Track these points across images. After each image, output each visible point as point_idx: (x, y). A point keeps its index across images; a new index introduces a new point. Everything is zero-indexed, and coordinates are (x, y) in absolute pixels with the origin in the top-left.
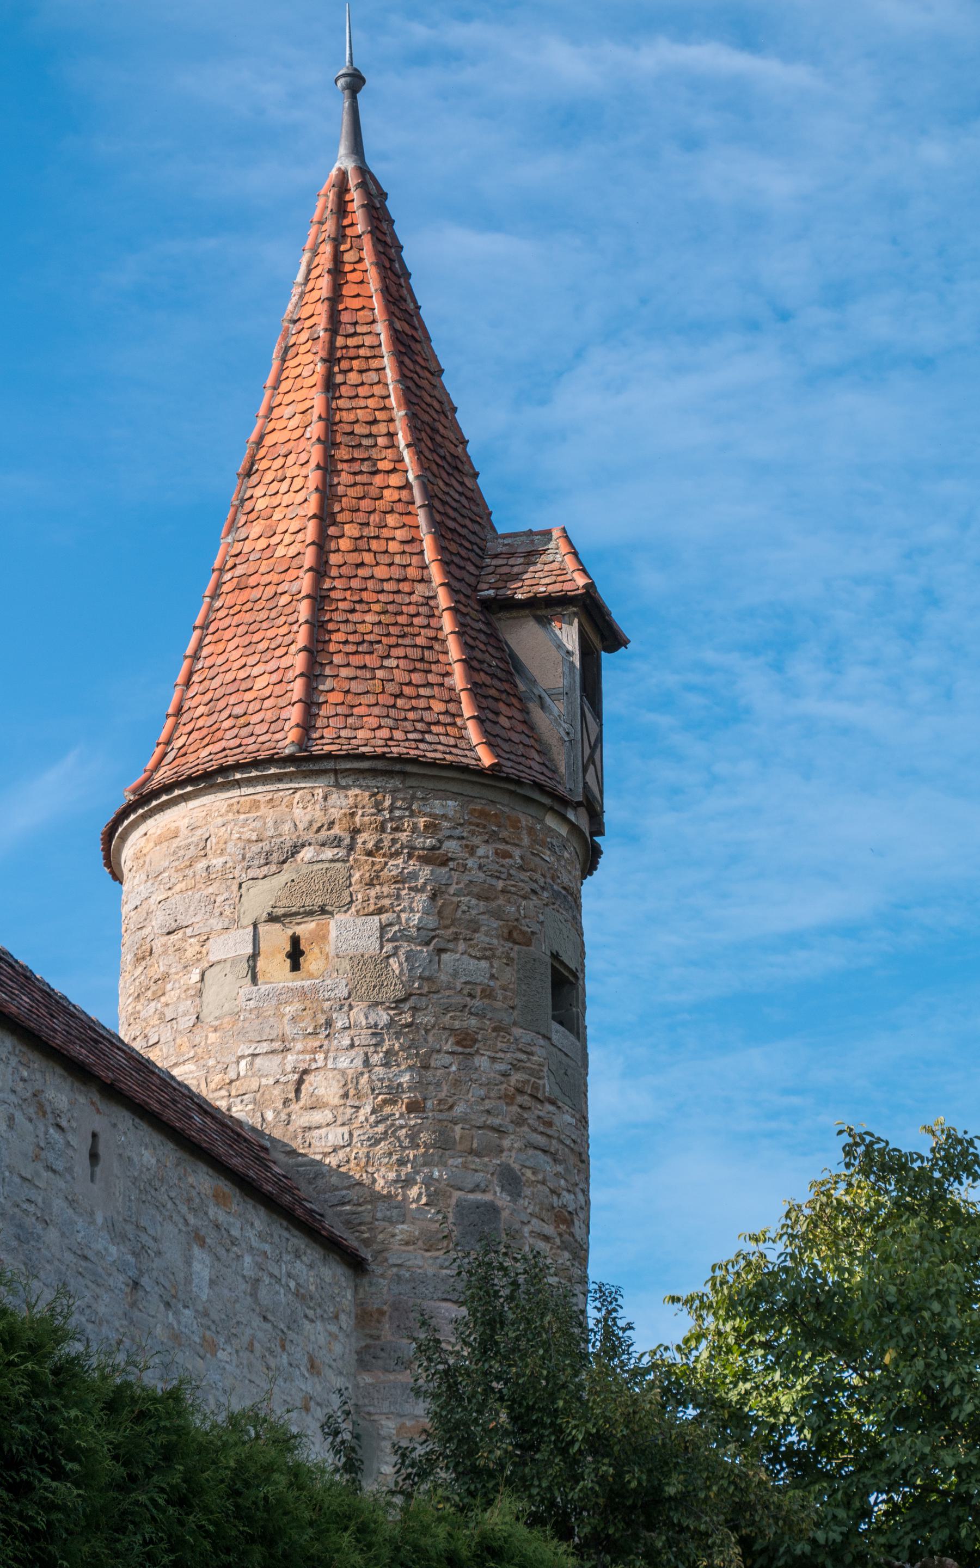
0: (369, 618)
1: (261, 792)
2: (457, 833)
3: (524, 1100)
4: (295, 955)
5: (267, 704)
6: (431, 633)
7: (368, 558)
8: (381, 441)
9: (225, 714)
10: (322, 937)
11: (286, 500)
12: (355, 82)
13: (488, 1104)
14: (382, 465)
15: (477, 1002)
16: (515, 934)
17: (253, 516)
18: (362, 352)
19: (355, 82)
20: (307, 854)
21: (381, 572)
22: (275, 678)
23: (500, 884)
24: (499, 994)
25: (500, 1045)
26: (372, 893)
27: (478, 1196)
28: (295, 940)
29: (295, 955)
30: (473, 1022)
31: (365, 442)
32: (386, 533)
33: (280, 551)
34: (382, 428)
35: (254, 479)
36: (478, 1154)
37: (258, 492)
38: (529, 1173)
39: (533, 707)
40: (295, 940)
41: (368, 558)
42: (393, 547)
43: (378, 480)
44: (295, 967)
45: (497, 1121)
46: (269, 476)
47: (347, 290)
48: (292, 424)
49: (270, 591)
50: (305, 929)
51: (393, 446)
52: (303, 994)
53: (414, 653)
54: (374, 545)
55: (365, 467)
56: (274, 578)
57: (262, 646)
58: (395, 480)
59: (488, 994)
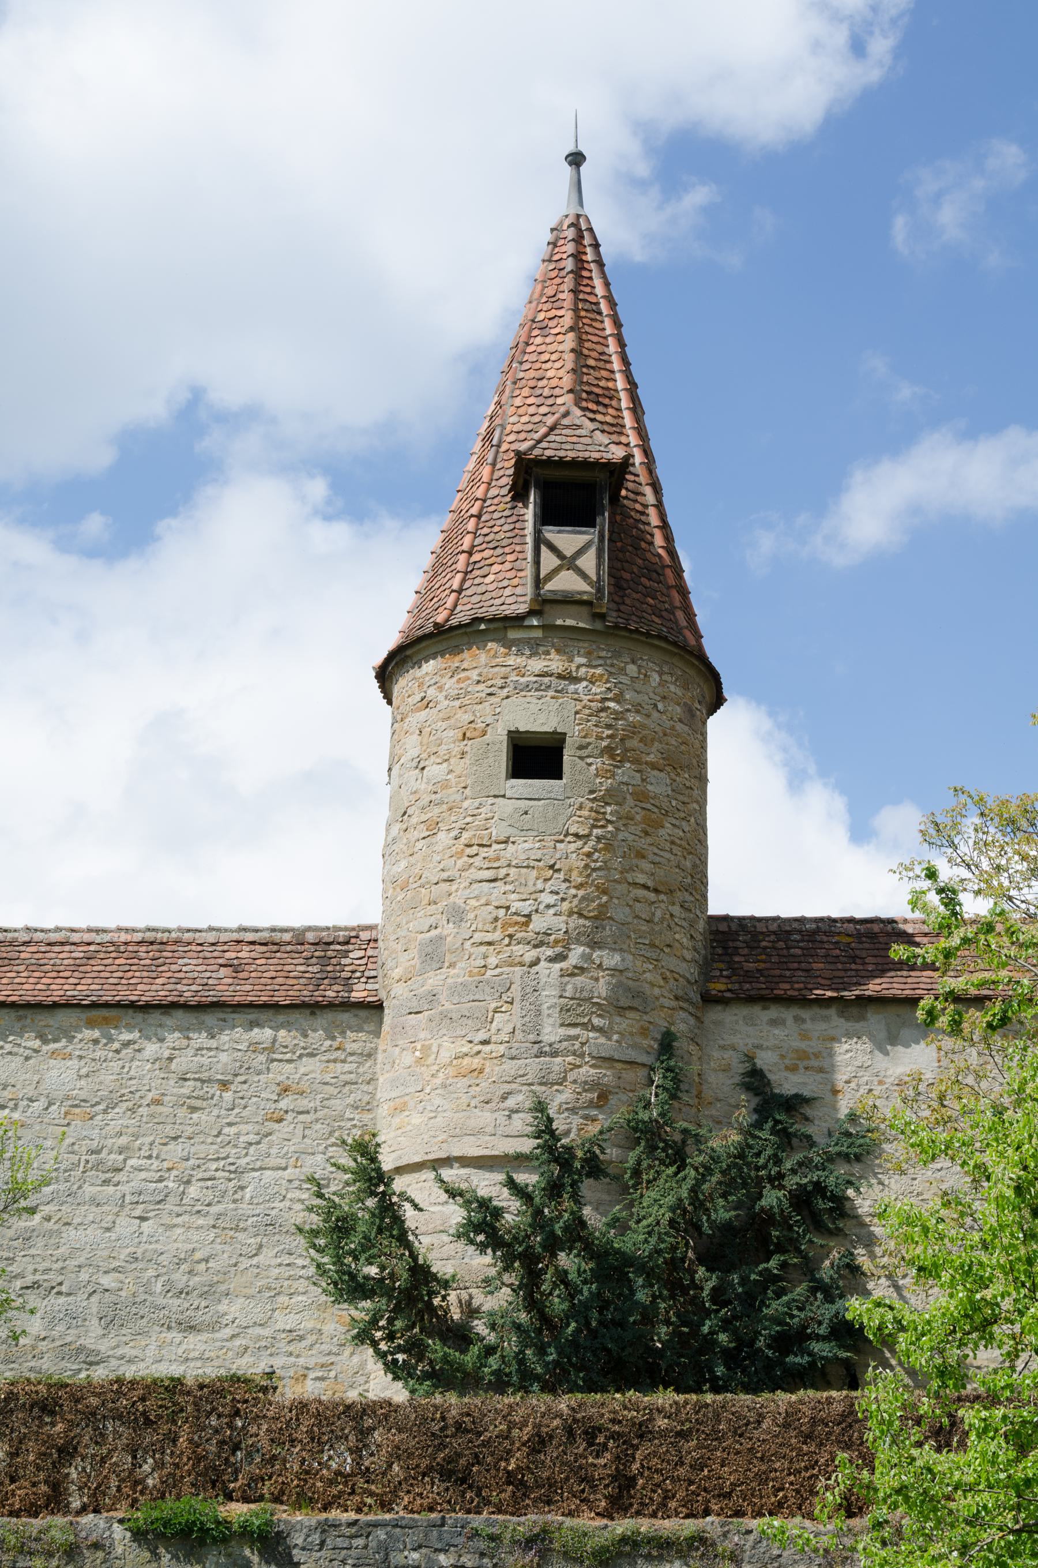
2: (433, 682)
3: (474, 850)
12: (576, 159)
13: (441, 866)
15: (438, 796)
16: (468, 735)
19: (576, 159)
23: (457, 703)
24: (454, 781)
25: (453, 819)
27: (434, 933)
30: (437, 810)
36: (435, 903)
38: (473, 903)
45: (445, 875)
59: (446, 785)
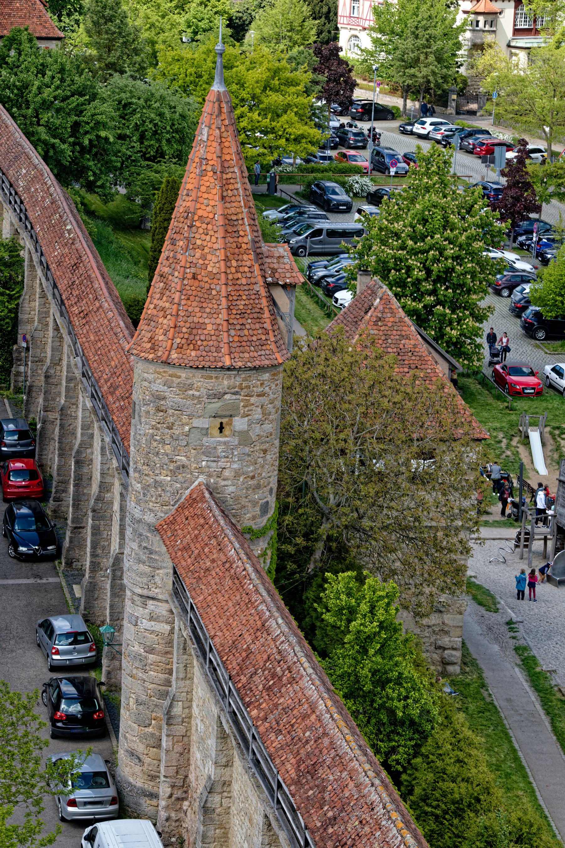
0: (243, 303)
1: (213, 374)
4: (221, 429)
5: (214, 338)
6: (259, 306)
7: (239, 275)
8: (240, 222)
9: (197, 338)
10: (230, 424)
11: (209, 245)
14: (242, 233)
17: (195, 246)
18: (232, 181)
20: (227, 397)
21: (244, 281)
22: (214, 327)
26: (247, 409)
28: (221, 423)
29: (221, 429)
31: (236, 223)
32: (244, 263)
33: (210, 269)
34: (240, 216)
35: (194, 229)
37: (197, 236)
39: (278, 318)
40: (221, 424)
41: (239, 275)
42: (246, 269)
43: (240, 239)
44: (221, 432)
46: (201, 231)
47: (225, 151)
48: (209, 209)
49: (207, 286)
50: (224, 420)
51: (243, 224)
52: (225, 443)
53: (255, 315)
54: (241, 269)
55: (236, 235)
56: (209, 281)
57: (208, 310)
58: (245, 240)
